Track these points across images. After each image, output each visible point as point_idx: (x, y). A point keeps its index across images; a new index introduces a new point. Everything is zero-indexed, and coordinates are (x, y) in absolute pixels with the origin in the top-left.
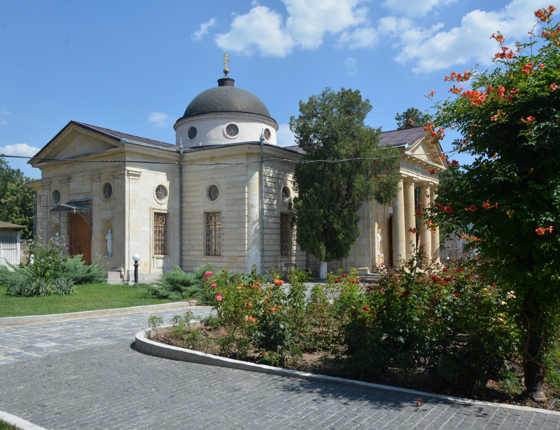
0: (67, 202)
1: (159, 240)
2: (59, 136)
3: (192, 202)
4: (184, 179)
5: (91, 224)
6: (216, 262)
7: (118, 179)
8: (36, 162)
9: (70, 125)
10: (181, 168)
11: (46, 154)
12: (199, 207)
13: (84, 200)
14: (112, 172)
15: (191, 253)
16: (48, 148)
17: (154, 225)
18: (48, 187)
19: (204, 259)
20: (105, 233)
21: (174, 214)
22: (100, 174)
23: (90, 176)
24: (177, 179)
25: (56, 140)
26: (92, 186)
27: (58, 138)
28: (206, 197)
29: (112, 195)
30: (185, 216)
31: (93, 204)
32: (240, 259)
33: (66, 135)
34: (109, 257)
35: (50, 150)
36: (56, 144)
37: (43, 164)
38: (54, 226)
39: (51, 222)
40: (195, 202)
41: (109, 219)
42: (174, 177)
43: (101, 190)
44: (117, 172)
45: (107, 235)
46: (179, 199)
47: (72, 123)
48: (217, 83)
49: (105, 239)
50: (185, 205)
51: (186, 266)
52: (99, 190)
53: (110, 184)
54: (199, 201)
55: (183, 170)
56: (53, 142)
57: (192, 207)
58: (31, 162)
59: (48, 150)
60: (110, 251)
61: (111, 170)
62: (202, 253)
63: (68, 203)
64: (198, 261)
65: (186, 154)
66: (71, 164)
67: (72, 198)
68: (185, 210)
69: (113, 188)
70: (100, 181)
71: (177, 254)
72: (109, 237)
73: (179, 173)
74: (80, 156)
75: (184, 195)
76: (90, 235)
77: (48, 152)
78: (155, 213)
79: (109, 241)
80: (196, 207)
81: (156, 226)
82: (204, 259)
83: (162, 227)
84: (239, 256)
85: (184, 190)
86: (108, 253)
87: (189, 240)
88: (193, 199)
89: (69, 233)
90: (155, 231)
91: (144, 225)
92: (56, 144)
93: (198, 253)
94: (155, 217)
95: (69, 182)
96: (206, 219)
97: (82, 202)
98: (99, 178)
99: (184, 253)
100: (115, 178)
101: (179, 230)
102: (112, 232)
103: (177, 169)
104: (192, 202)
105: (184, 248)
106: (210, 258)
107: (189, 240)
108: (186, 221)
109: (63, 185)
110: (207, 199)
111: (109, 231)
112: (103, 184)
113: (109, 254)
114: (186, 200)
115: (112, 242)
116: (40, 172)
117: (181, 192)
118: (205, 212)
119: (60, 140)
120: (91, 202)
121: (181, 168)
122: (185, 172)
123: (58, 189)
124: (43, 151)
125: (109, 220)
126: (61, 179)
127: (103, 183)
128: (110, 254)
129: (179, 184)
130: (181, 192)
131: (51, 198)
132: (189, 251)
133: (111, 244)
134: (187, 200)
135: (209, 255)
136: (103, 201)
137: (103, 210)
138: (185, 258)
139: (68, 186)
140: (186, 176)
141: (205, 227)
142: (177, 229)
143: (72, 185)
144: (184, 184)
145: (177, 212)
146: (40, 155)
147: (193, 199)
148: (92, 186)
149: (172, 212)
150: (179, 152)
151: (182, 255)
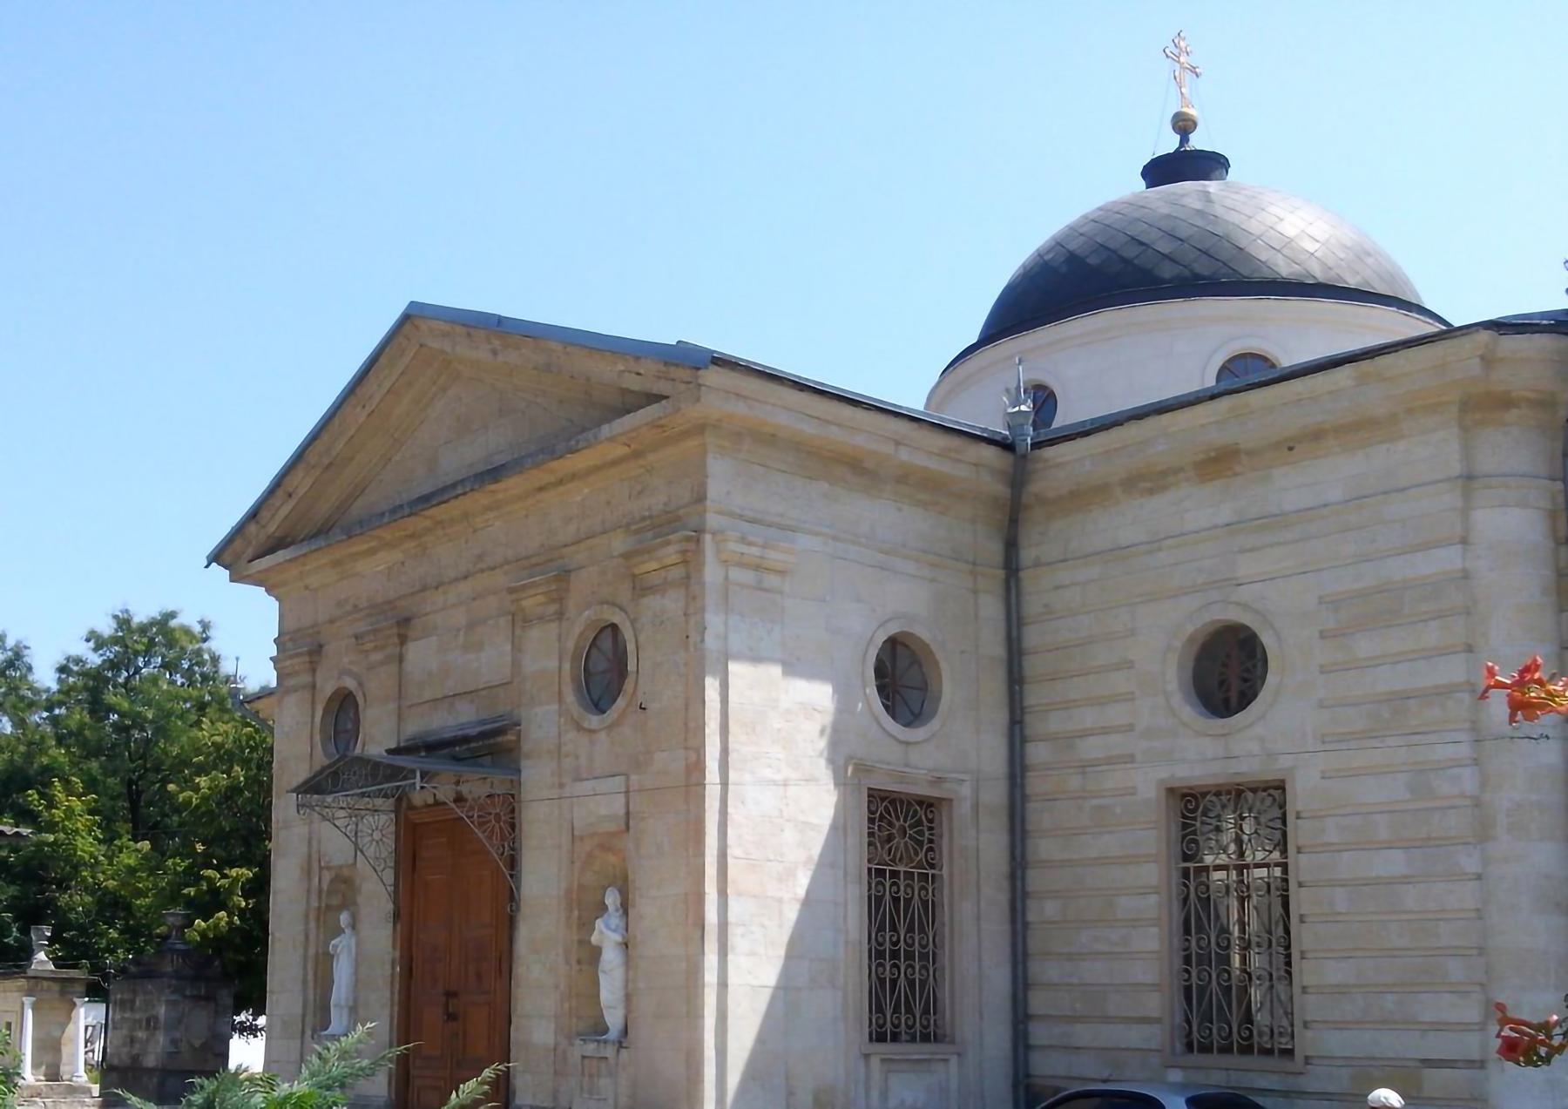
0: (393, 745)
1: (895, 955)
3: (1085, 734)
4: (1032, 605)
5: (513, 863)
10: (1011, 546)
12: (1131, 759)
14: (627, 556)
17: (866, 865)
20: (586, 910)
21: (976, 807)
22: (564, 575)
23: (511, 591)
24: (991, 607)
26: (517, 648)
28: (1177, 699)
29: (629, 685)
30: (1039, 816)
31: (526, 747)
34: (609, 1052)
37: (281, 556)
38: (327, 876)
39: (315, 856)
40: (1105, 731)
41: (612, 827)
42: (975, 592)
43: (567, 666)
45: (599, 924)
46: (1001, 717)
48: (1142, 184)
49: (584, 943)
50: (1037, 753)
52: (554, 664)
53: (614, 628)
54: (1130, 728)
55: (1027, 554)
57: (1083, 768)
60: (614, 1019)
61: (619, 543)
63: (390, 752)
66: (410, 545)
67: (417, 725)
68: (1036, 784)
69: (631, 647)
70: (560, 615)
72: (606, 934)
73: (1001, 573)
74: (454, 486)
75: (1034, 696)
76: (509, 924)
79: (611, 957)
80: (1110, 761)
81: (880, 873)
83: (909, 875)
85: (1033, 666)
86: (600, 1029)
87: (1070, 957)
88: (1088, 718)
89: (397, 916)
90: (875, 903)
94: (871, 821)
95: (403, 640)
97: (465, 740)
98: (559, 598)
100: (641, 589)
101: (1003, 898)
102: (625, 907)
103: (993, 549)
104: (1085, 734)
105: (1038, 1002)
107: (1070, 957)
108: (1043, 848)
109: (376, 657)
111: (612, 899)
112: (577, 630)
113: (606, 1030)
114: (1045, 724)
115: (628, 963)
117: (1015, 680)
120: (511, 737)
121: (1011, 546)
122: (1037, 564)
123: (350, 684)
125: (613, 835)
126: (362, 627)
127: (581, 621)
128: (613, 1033)
129: (1000, 636)
130: (1015, 680)
131: (317, 738)
133: (619, 973)
134: (1055, 723)
136: (579, 727)
137: (579, 779)
139: (401, 659)
140: (1037, 591)
142: (995, 896)
143: (421, 655)
144: (1032, 637)
145: (995, 794)
147: (1088, 718)
148: (517, 648)
149: (966, 791)
150: (1006, 445)
151: (1028, 1047)
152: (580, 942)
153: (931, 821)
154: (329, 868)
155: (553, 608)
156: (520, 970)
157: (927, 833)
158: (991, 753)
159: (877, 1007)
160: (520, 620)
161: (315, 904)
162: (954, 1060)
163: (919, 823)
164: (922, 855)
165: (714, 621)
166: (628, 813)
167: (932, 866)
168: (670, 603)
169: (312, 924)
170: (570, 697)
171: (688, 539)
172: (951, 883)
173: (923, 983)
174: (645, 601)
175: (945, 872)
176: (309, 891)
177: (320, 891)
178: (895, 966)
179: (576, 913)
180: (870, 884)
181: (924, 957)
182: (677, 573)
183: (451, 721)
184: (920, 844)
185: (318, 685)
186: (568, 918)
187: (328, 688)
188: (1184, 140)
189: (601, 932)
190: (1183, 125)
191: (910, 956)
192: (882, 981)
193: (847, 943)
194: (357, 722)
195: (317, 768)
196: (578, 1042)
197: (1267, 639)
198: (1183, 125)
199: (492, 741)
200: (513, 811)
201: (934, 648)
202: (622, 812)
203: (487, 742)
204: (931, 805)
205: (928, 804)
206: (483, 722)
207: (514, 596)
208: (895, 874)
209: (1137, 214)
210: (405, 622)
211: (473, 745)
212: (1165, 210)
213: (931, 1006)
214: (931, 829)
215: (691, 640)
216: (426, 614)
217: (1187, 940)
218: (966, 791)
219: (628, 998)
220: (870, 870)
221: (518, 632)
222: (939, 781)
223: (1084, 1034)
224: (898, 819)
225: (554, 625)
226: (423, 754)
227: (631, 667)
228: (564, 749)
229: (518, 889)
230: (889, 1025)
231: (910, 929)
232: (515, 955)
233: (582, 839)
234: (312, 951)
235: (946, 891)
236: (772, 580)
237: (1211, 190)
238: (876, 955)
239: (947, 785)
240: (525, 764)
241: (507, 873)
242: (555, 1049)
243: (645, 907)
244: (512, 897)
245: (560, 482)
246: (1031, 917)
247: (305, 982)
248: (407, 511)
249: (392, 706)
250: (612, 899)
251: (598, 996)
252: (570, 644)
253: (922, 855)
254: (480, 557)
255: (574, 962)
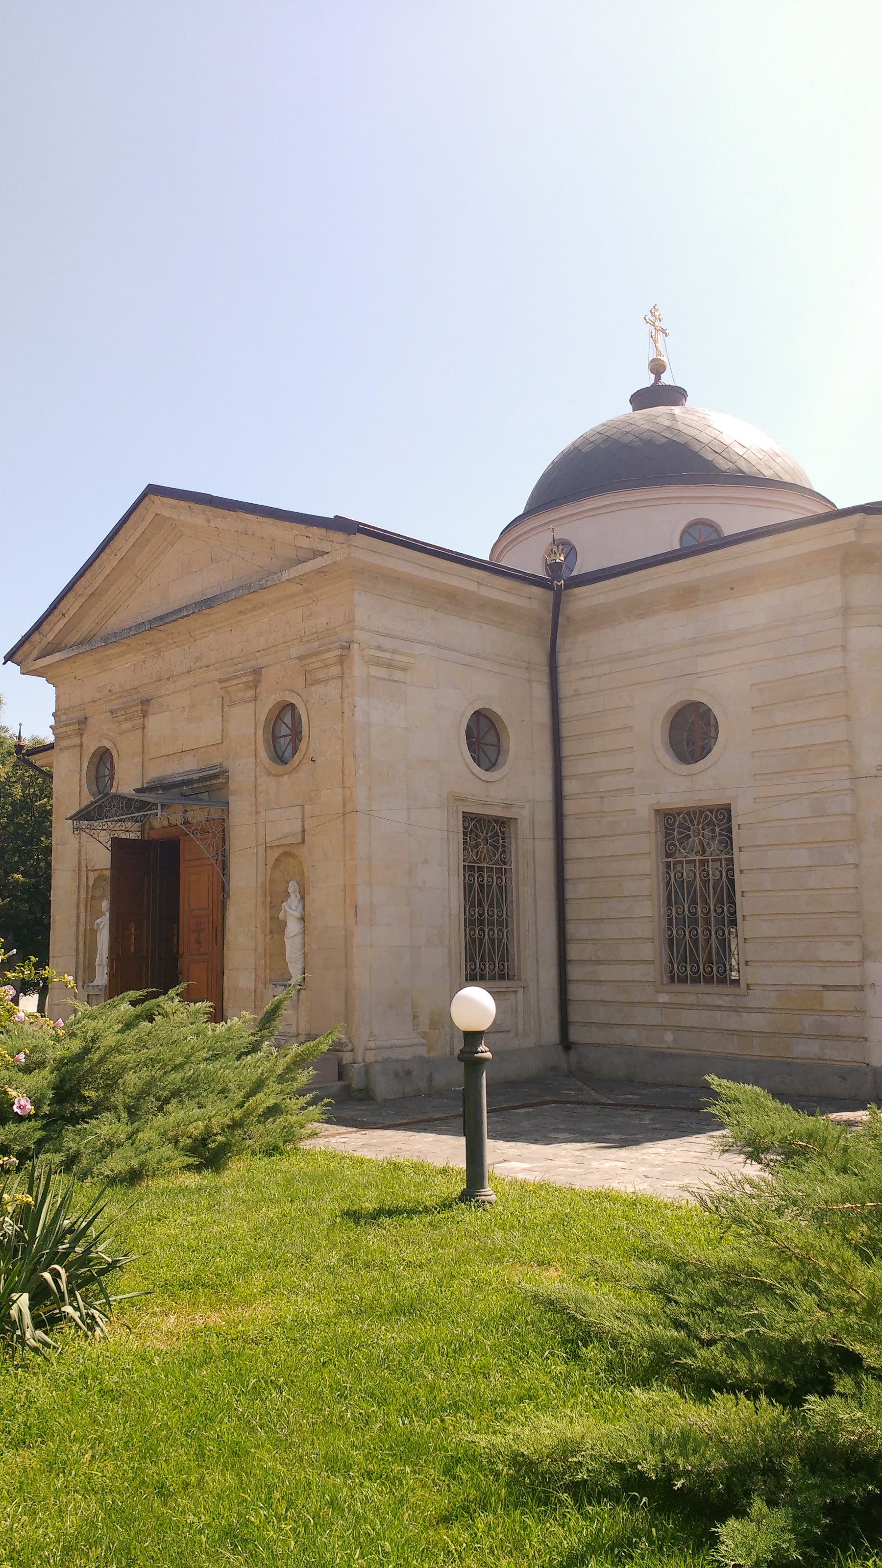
0: (139, 786)
1: (481, 922)
2: (108, 550)
3: (602, 774)
4: (565, 690)
5: (225, 866)
6: (719, 1008)
7: (325, 681)
8: (35, 653)
9: (146, 500)
11: (64, 621)
13: (196, 776)
14: (300, 658)
15: (604, 972)
16: (71, 595)
17: (462, 864)
18: (76, 741)
19: (663, 998)
21: (533, 823)
22: (257, 672)
23: (221, 681)
24: (541, 691)
25: (96, 565)
27: (103, 556)
29: (303, 746)
31: (232, 786)
32: (832, 1000)
33: (132, 540)
35: (77, 605)
36: (96, 578)
38: (92, 876)
39: (83, 863)
40: (615, 772)
42: (530, 681)
43: (260, 732)
44: (316, 654)
46: (547, 765)
47: (152, 490)
49: (274, 919)
50: (569, 787)
51: (586, 1024)
53: (292, 706)
56: (88, 575)
58: (19, 656)
59: (71, 606)
61: (295, 652)
62: (651, 973)
63: (136, 790)
64: (633, 1004)
65: (577, 590)
67: (155, 772)
71: (549, 976)
72: (291, 909)
74: (180, 610)
75: (567, 749)
77: (73, 611)
78: (467, 817)
79: (293, 927)
82: (663, 998)
84: (826, 987)
85: (566, 730)
90: (468, 888)
91: (426, 862)
92: (100, 579)
93: (636, 973)
94: (465, 834)
95: (145, 714)
96: (661, 838)
98: (256, 685)
99: (574, 972)
105: (573, 952)
106: (690, 993)
109: (126, 725)
110: (668, 760)
111: (292, 887)
116: (51, 690)
118: (657, 811)
119: (109, 561)
123: (107, 744)
124: (56, 612)
126: (115, 705)
127: (268, 702)
131: (84, 781)
132: (598, 962)
133: (298, 940)
135: (683, 980)
136: (269, 773)
138: (575, 992)
141: (662, 868)
143: (157, 725)
144: (566, 710)
145: (546, 814)
146: (45, 627)
152: (271, 918)
153: (503, 833)
154: (94, 871)
155: (251, 693)
156: (230, 937)
157: (501, 841)
158: (544, 789)
159: (470, 958)
160: (227, 702)
161: (83, 895)
162: (521, 990)
163: (496, 834)
164: (498, 856)
165: (361, 702)
166: (303, 831)
167: (505, 863)
168: (332, 690)
169: (82, 909)
170: (263, 754)
171: (342, 647)
172: (517, 874)
173: (500, 941)
174: (313, 688)
175: (513, 866)
176: (79, 887)
177: (87, 886)
178: (482, 930)
179: (269, 899)
180: (464, 875)
181: (501, 923)
182: (335, 670)
183: (180, 770)
184: (497, 849)
185: (85, 746)
186: (264, 902)
187: (91, 746)
188: (658, 378)
189: (286, 911)
190: (657, 368)
191: (491, 923)
192: (473, 940)
193: (450, 916)
194: (112, 769)
195: (85, 803)
196: (271, 986)
197: (717, 712)
198: (657, 368)
199: (208, 783)
200: (223, 830)
201: (504, 718)
202: (300, 829)
203: (205, 784)
204: (503, 823)
205: (502, 822)
206: (203, 770)
207: (224, 685)
208: (480, 869)
209: (627, 429)
210: (146, 702)
211: (195, 786)
212: (646, 427)
213: (505, 957)
214: (503, 838)
215: (346, 715)
216: (162, 697)
217: (670, 909)
218: (526, 813)
219: (305, 955)
220: (464, 866)
221: (226, 709)
222: (508, 806)
223: (604, 972)
224: (482, 833)
225: (251, 705)
226: (160, 792)
227: (305, 732)
228: (259, 788)
229: (229, 882)
230: (478, 969)
231: (491, 905)
232: (227, 928)
233: (272, 847)
234: (82, 928)
235: (514, 880)
236: (398, 675)
237: (676, 412)
238: (469, 922)
239: (513, 810)
240: (232, 799)
241: (220, 872)
242: (255, 991)
243: (316, 895)
244: (224, 889)
245: (255, 608)
246: (569, 895)
247: (77, 949)
248: (147, 627)
249: (138, 760)
250: (292, 887)
251: (284, 954)
252: (263, 718)
253: (498, 856)
254: (198, 659)
255: (268, 932)
